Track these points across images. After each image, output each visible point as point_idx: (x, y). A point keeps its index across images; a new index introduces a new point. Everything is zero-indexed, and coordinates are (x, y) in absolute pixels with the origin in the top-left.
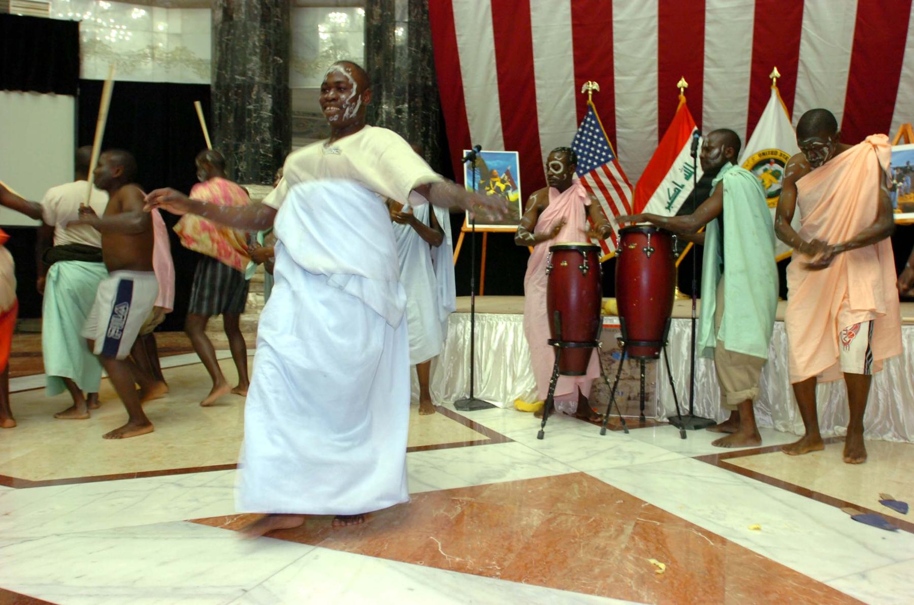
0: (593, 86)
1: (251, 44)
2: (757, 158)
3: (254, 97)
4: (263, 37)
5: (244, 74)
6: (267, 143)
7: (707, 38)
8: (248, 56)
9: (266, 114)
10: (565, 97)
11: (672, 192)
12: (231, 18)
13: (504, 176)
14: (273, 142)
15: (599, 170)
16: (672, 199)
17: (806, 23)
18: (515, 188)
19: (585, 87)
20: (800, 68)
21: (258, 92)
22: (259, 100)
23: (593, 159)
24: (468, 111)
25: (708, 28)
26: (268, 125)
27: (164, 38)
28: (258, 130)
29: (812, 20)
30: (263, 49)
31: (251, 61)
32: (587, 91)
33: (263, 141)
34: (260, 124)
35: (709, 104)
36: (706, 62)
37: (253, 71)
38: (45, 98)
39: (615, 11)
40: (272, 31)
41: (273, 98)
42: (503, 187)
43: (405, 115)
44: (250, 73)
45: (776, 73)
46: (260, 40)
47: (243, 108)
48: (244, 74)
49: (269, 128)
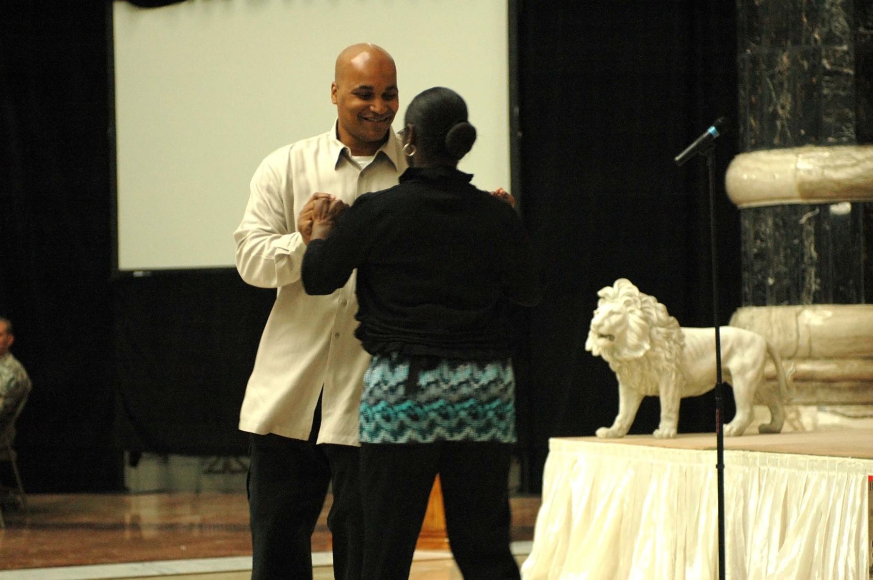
6: (841, 43)
14: (856, 37)
33: (830, 39)
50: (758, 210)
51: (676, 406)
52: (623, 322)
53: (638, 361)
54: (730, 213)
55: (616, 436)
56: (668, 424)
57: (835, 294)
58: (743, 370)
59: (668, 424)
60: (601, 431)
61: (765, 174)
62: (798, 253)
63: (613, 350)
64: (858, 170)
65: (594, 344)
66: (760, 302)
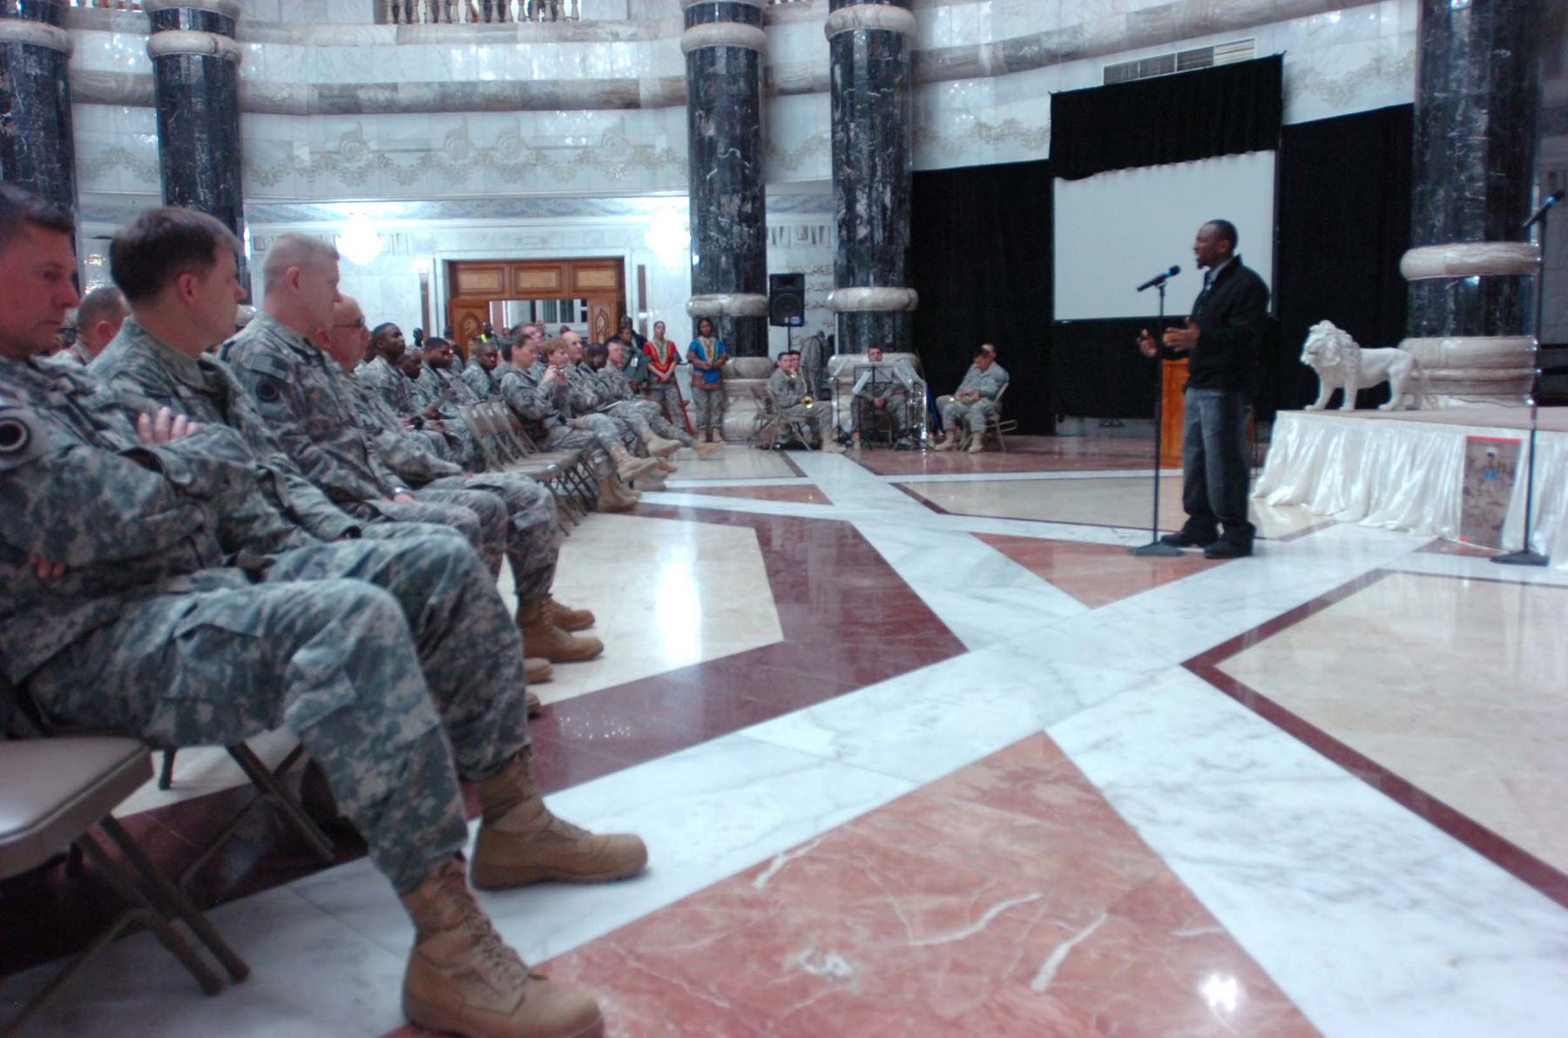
1: (1456, 43)
3: (1459, 118)
4: (1475, 28)
5: (1445, 89)
8: (1452, 62)
9: (1477, 139)
12: (1432, 11)
14: (1488, 178)
21: (1466, 110)
22: (1467, 121)
26: (1480, 154)
27: (1394, 43)
28: (1462, 166)
30: (1475, 44)
31: (1456, 67)
33: (1471, 179)
34: (1466, 155)
37: (1459, 81)
38: (1243, 157)
40: (1491, 14)
41: (1491, 113)
44: (1454, 85)
46: (1471, 34)
47: (1443, 137)
48: (1445, 89)
49: (1482, 159)
50: (1419, 284)
51: (1354, 394)
52: (1324, 346)
53: (1332, 368)
54: (1401, 285)
55: (1318, 410)
56: (1349, 403)
57: (1464, 330)
58: (1397, 374)
59: (1349, 403)
60: (1308, 407)
61: (1423, 261)
62: (1441, 309)
63: (1317, 361)
64: (1484, 257)
65: (1305, 358)
66: (1417, 335)
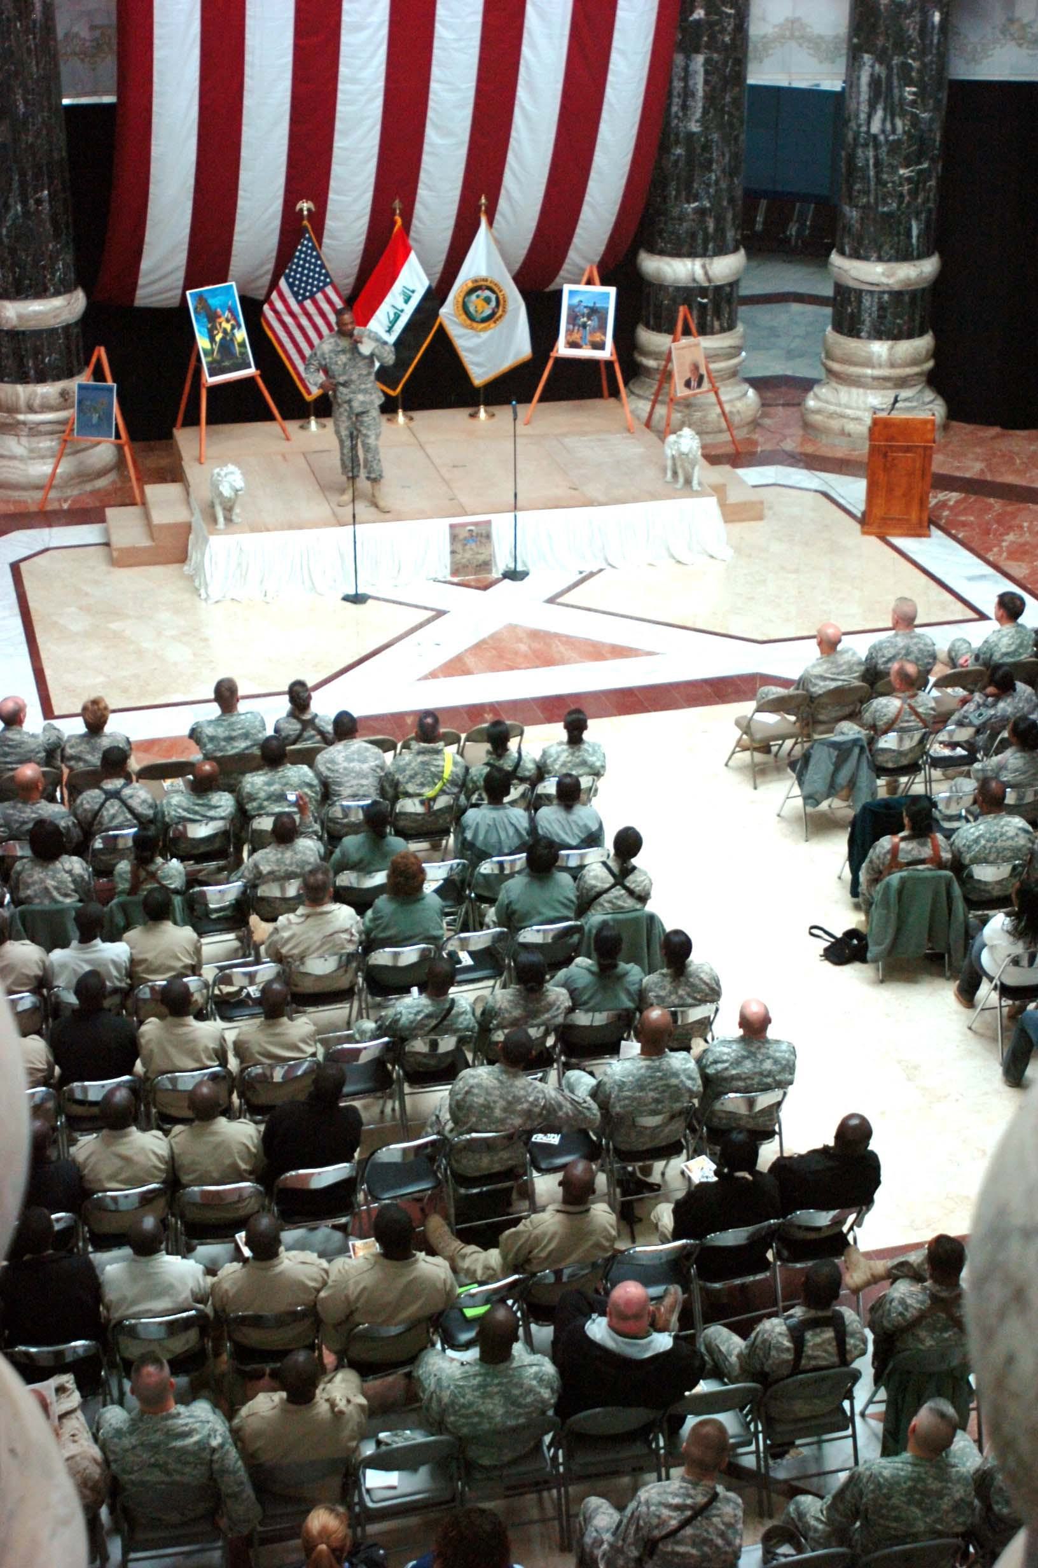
0: (305, 206)
2: (470, 285)
7: (423, 165)
10: (271, 210)
11: (392, 317)
13: (227, 314)
15: (319, 296)
16: (393, 323)
17: (511, 157)
18: (239, 326)
19: (298, 207)
20: (503, 192)
23: (312, 285)
24: (149, 217)
25: (425, 158)
29: (516, 156)
32: (301, 210)
35: (420, 221)
36: (420, 185)
39: (337, 137)
42: (228, 327)
43: (46, 205)
45: (483, 200)
